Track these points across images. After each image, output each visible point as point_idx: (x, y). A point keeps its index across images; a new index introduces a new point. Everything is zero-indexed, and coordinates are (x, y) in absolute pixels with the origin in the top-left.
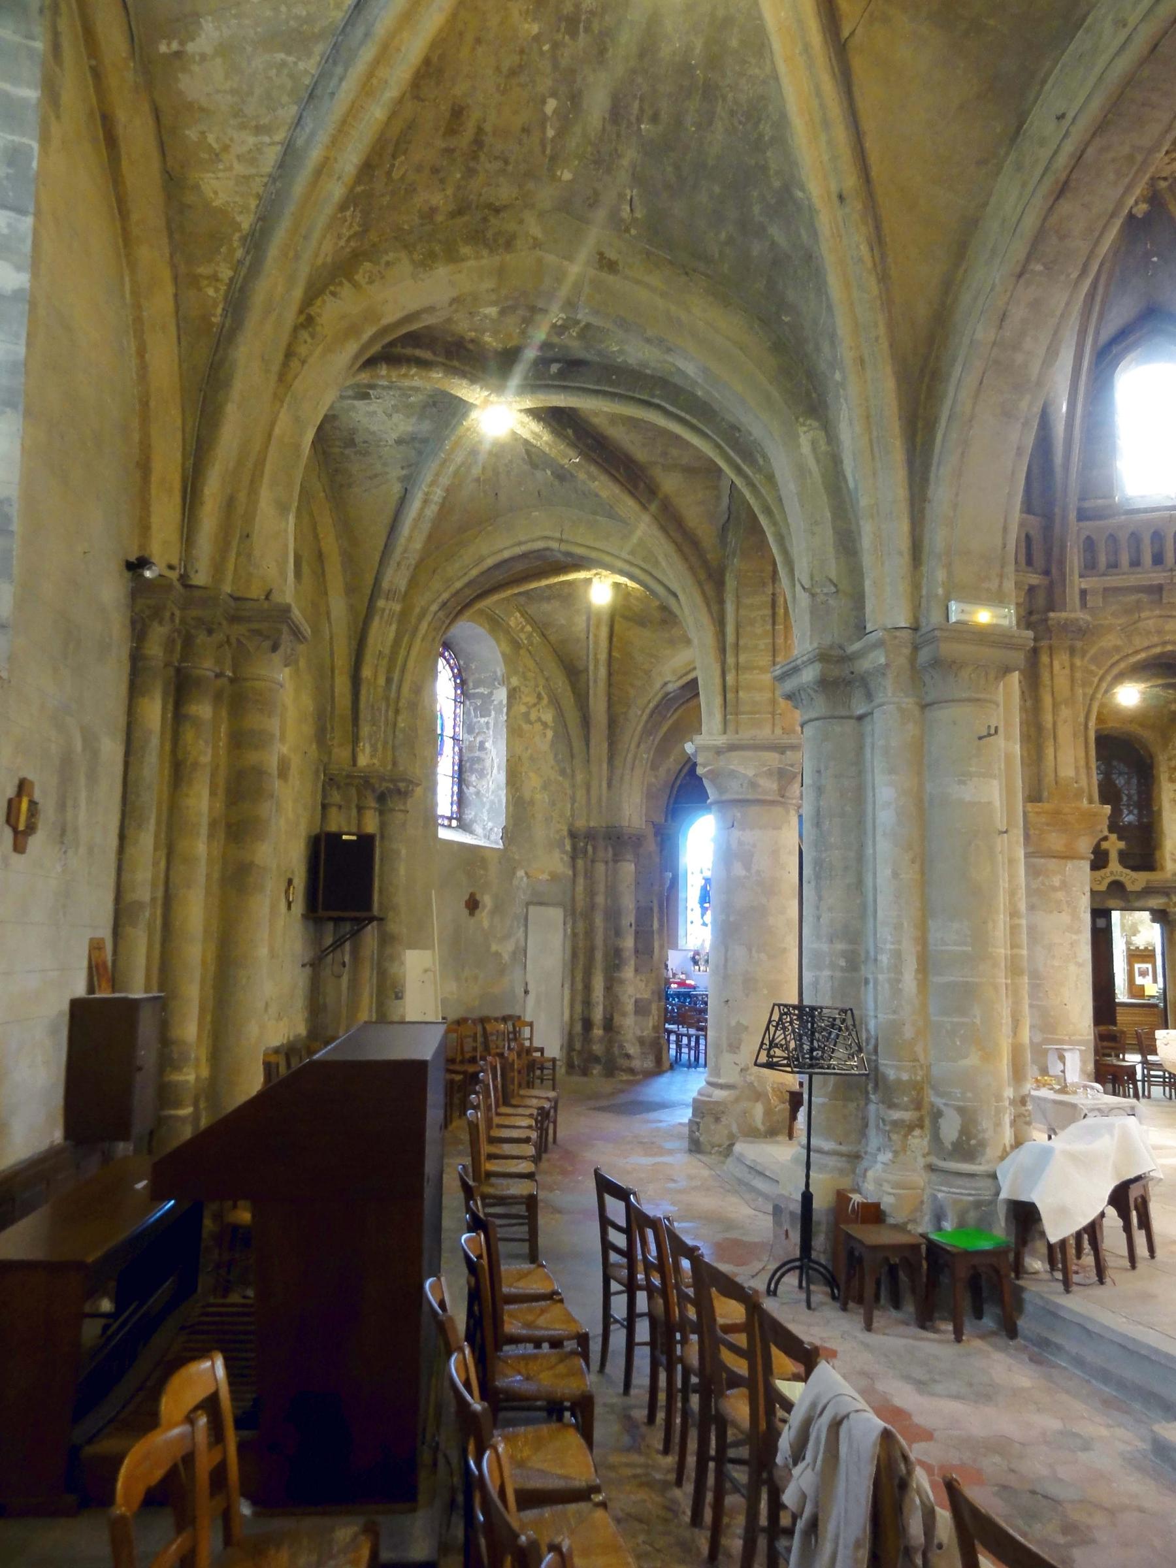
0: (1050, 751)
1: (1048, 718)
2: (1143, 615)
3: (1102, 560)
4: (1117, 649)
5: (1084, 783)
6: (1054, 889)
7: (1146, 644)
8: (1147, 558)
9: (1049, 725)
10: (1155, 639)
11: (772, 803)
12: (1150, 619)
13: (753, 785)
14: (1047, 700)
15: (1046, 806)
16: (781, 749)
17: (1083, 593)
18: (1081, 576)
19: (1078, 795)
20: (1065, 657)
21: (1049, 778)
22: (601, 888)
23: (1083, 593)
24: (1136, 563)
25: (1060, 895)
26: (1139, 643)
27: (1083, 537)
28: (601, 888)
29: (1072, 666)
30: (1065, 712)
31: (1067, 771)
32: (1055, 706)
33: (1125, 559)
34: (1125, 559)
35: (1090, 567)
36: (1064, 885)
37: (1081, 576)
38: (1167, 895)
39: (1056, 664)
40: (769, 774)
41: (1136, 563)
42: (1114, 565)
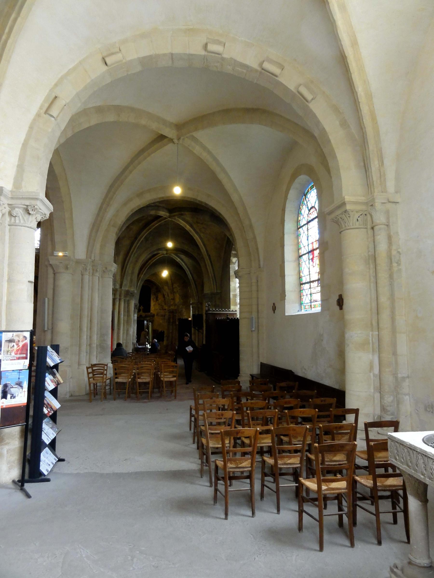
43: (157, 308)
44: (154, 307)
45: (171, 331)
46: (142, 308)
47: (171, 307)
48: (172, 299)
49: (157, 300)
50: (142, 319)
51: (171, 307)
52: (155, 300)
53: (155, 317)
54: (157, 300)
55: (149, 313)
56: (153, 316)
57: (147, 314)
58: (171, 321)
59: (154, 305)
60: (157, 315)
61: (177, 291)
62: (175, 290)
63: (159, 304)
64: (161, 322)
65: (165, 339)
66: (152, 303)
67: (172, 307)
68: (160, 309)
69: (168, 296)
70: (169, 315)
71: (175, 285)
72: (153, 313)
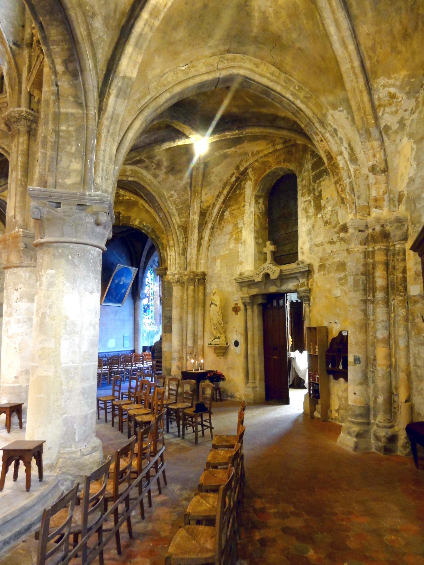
5: (18, 218)
38: (297, 278)
43: (320, 239)
44: (310, 235)
45: (381, 334)
46: (269, 248)
47: (375, 213)
48: (373, 169)
49: (319, 208)
50: (273, 289)
51: (375, 213)
52: (312, 210)
53: (317, 275)
54: (319, 208)
55: (293, 265)
56: (308, 273)
57: (284, 267)
58: (380, 281)
59: (309, 232)
60: (322, 267)
61: (402, 123)
62: (388, 118)
63: (327, 223)
64: (338, 292)
65: (353, 372)
66: (303, 225)
67: (383, 213)
68: (332, 242)
69: (354, 159)
70: (366, 255)
71: (386, 86)
72: (308, 261)
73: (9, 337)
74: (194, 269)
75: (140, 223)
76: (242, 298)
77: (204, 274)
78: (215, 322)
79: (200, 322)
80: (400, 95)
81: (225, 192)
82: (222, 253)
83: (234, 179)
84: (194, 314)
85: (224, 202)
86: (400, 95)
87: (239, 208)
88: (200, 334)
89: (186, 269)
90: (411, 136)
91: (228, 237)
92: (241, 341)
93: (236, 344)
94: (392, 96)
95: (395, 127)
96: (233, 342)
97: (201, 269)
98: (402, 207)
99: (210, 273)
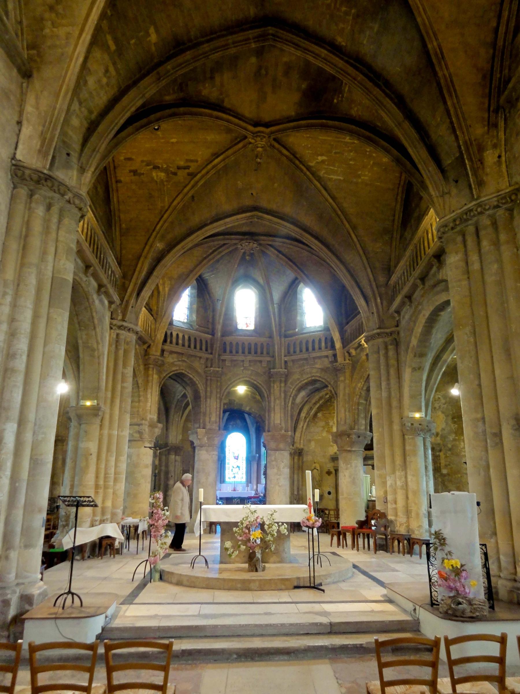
0: (272, 415)
1: (272, 404)
2: (306, 367)
3: (292, 350)
4: (298, 379)
5: (283, 425)
6: (272, 461)
7: (307, 376)
8: (304, 350)
9: (272, 406)
10: (310, 376)
11: (139, 440)
12: (307, 369)
13: (133, 436)
14: (272, 399)
15: (270, 433)
16: (139, 425)
17: (286, 362)
18: (285, 356)
19: (281, 429)
20: (278, 384)
21: (272, 424)
22: (164, 464)
23: (286, 362)
24: (301, 351)
25: (274, 463)
26: (305, 377)
27: (287, 344)
28: (164, 464)
29: (280, 387)
30: (278, 402)
31: (278, 421)
32: (275, 400)
33: (298, 350)
34: (298, 350)
35: (288, 353)
36: (275, 460)
37: (285, 356)
39: (275, 386)
40: (136, 432)
41: (301, 351)
42: (295, 352)
61: (440, 407)
73: (280, 486)
74: (298, 446)
75: (250, 409)
76: (334, 467)
77: (302, 449)
78: (317, 480)
79: (300, 479)
80: (442, 398)
81: (321, 402)
82: (316, 437)
83: (328, 396)
84: (298, 474)
85: (318, 408)
86: (442, 398)
87: (330, 413)
88: (300, 487)
89: (293, 446)
90: (443, 412)
91: (321, 429)
92: (333, 491)
93: (329, 493)
94: (439, 398)
95: (437, 408)
96: (327, 492)
97: (302, 447)
98: (438, 438)
99: (306, 449)
